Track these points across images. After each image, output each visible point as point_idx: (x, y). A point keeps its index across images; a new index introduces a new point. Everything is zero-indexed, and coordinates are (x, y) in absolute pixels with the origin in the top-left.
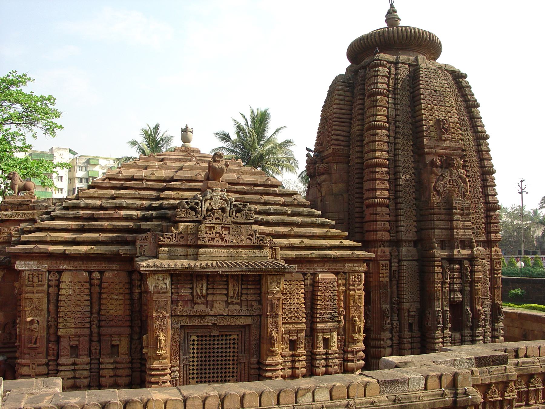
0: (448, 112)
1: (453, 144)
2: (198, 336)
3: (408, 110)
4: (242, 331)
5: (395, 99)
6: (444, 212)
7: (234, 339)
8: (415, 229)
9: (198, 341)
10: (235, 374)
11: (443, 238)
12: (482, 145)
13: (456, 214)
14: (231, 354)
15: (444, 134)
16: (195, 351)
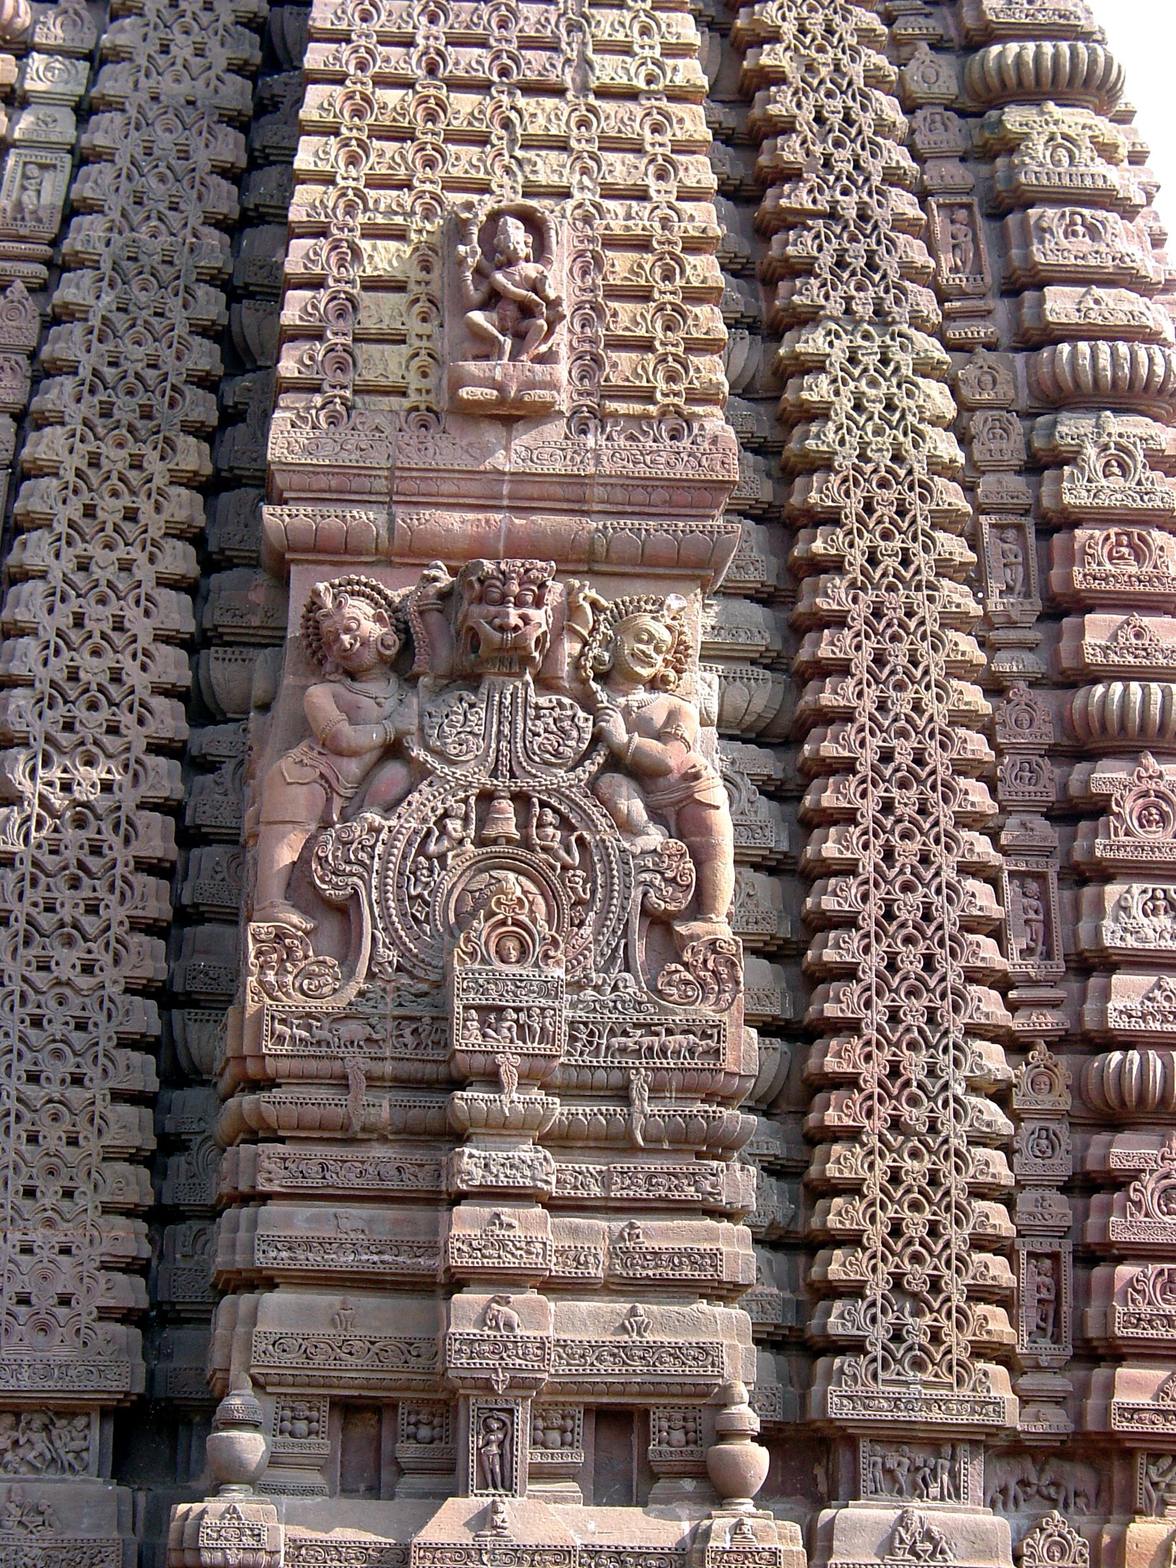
0: (611, 144)
1: (608, 454)
3: (202, 158)
5: (96, 59)
6: (382, 1108)
8: (130, 1292)
11: (355, 1373)
12: (1072, 458)
13: (504, 1128)
15: (486, 348)
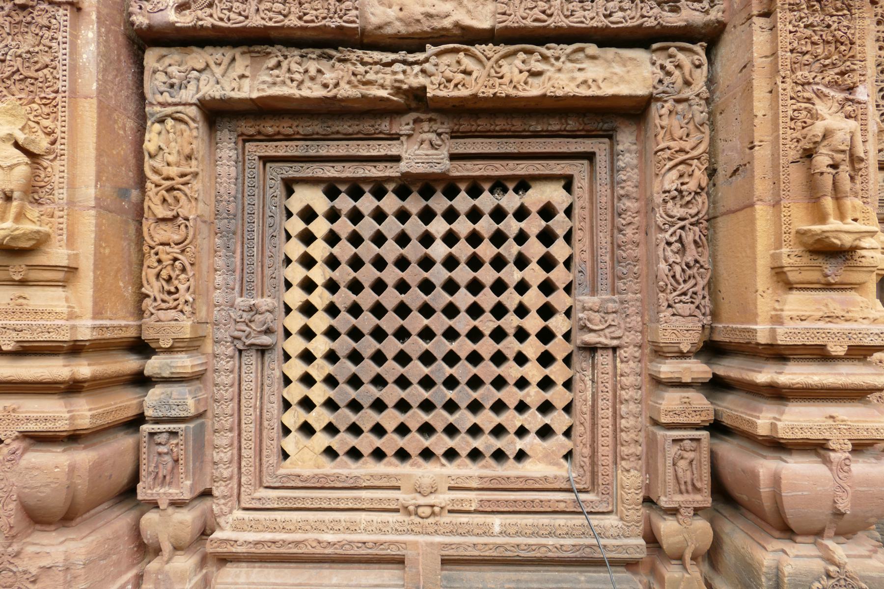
2: (332, 193)
4: (589, 157)
7: (547, 212)
9: (333, 216)
10: (558, 420)
14: (534, 299)
16: (319, 274)
